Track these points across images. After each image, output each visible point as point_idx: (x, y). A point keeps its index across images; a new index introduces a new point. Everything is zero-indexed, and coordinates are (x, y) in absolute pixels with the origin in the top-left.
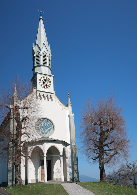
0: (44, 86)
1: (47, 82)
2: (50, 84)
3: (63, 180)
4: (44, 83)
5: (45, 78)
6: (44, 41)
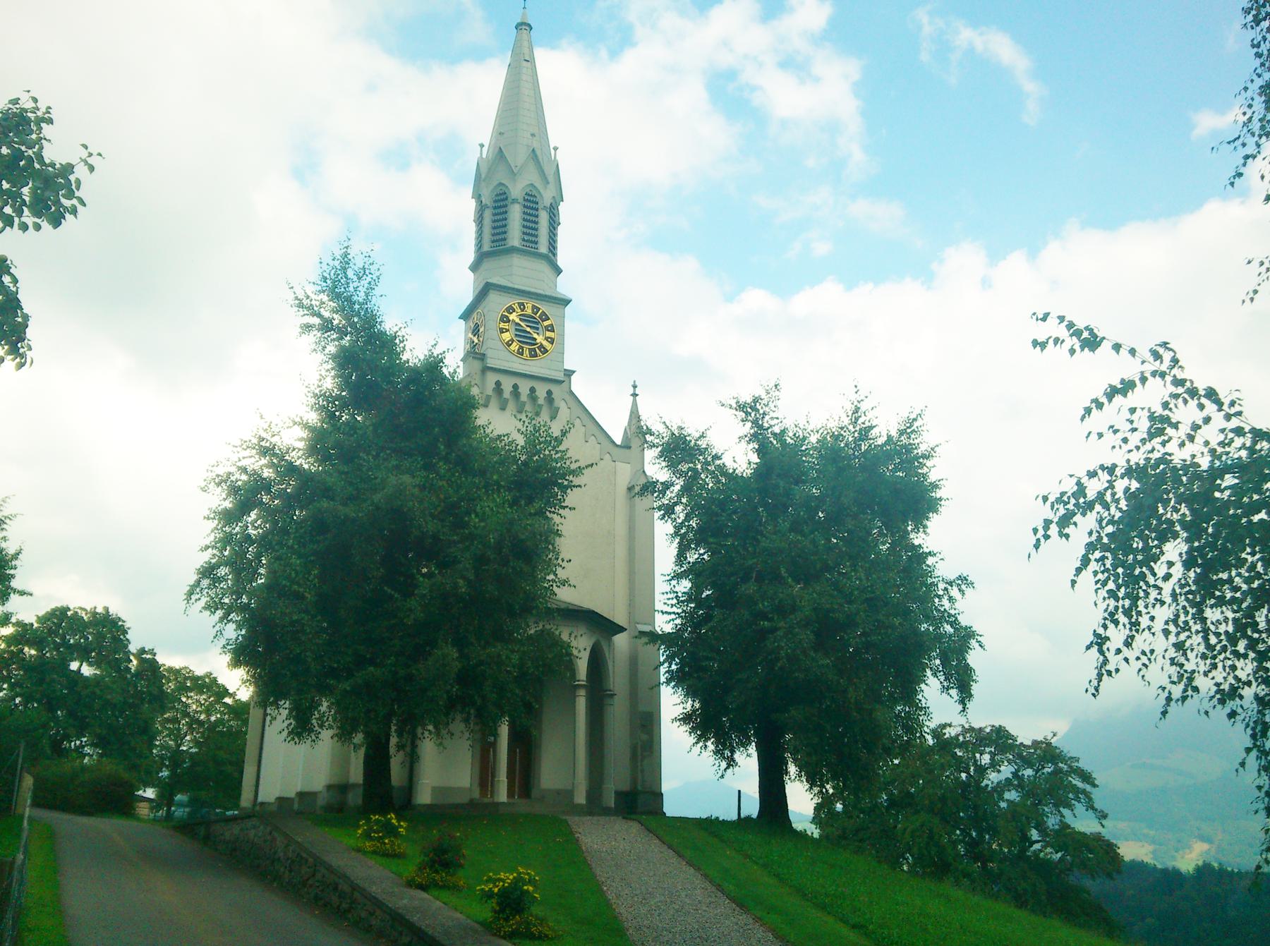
0: (521, 348)
1: (537, 329)
2: (547, 339)
3: (581, 798)
4: (520, 333)
5: (529, 311)
6: (533, 135)
